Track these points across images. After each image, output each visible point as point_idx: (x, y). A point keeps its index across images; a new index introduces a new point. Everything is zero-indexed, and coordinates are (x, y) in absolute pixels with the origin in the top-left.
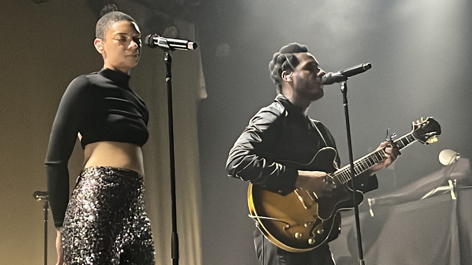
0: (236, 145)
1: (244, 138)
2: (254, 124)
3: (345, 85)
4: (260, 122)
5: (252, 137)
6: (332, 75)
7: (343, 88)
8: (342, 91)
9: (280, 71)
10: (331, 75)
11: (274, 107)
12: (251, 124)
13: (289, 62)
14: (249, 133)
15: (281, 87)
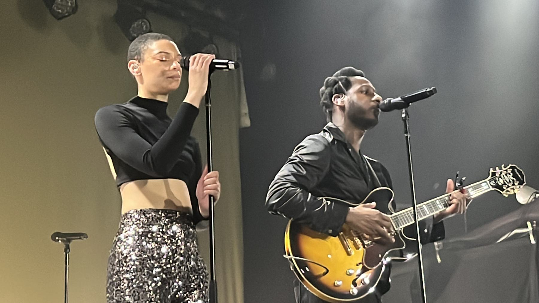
1: (286, 169)
2: (298, 154)
3: (407, 113)
4: (304, 151)
5: (294, 168)
6: (392, 101)
7: (404, 115)
10: (390, 101)
11: (322, 135)
12: (294, 155)
13: (342, 85)
14: (291, 165)
15: (331, 113)
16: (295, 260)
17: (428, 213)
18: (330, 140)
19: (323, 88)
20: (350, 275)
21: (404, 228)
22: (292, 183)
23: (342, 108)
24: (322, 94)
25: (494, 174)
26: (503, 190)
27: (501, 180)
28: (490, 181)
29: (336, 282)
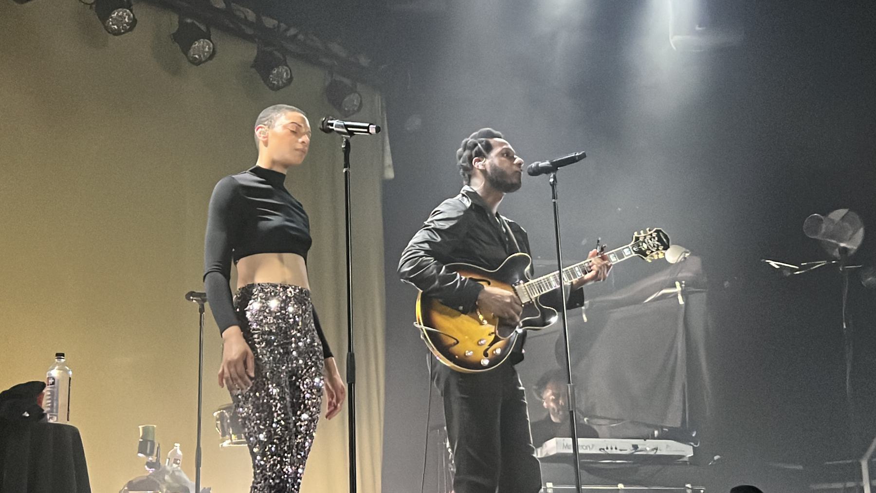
0: (410, 244)
1: (421, 236)
9: (470, 159)
12: (429, 220)
15: (470, 177)
18: (468, 204)
19: (460, 150)
20: (482, 345)
21: (541, 296)
22: (426, 251)
23: (484, 172)
24: (460, 157)
25: (637, 239)
26: (646, 255)
27: (645, 246)
28: (633, 246)
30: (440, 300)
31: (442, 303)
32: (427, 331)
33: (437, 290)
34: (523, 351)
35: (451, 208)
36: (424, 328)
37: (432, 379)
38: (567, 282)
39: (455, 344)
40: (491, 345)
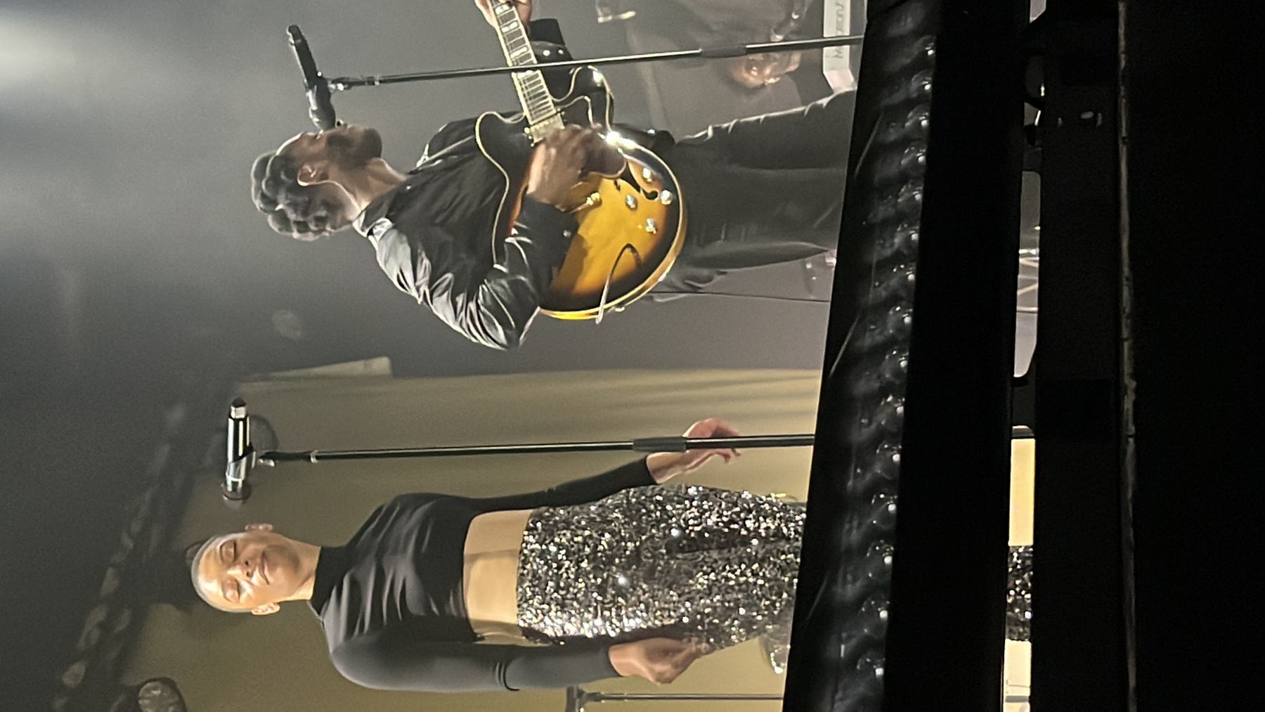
0: (457, 328)
1: (442, 309)
8: (349, 88)
12: (414, 293)
14: (435, 300)
16: (607, 302)
17: (524, 49)
20: (636, 202)
22: (469, 299)
29: (648, 229)
30: (555, 270)
31: (560, 268)
32: (607, 302)
33: (536, 282)
34: (652, 132)
35: (393, 258)
36: (603, 306)
37: (695, 290)
38: (527, 48)
39: (633, 250)
40: (638, 188)
